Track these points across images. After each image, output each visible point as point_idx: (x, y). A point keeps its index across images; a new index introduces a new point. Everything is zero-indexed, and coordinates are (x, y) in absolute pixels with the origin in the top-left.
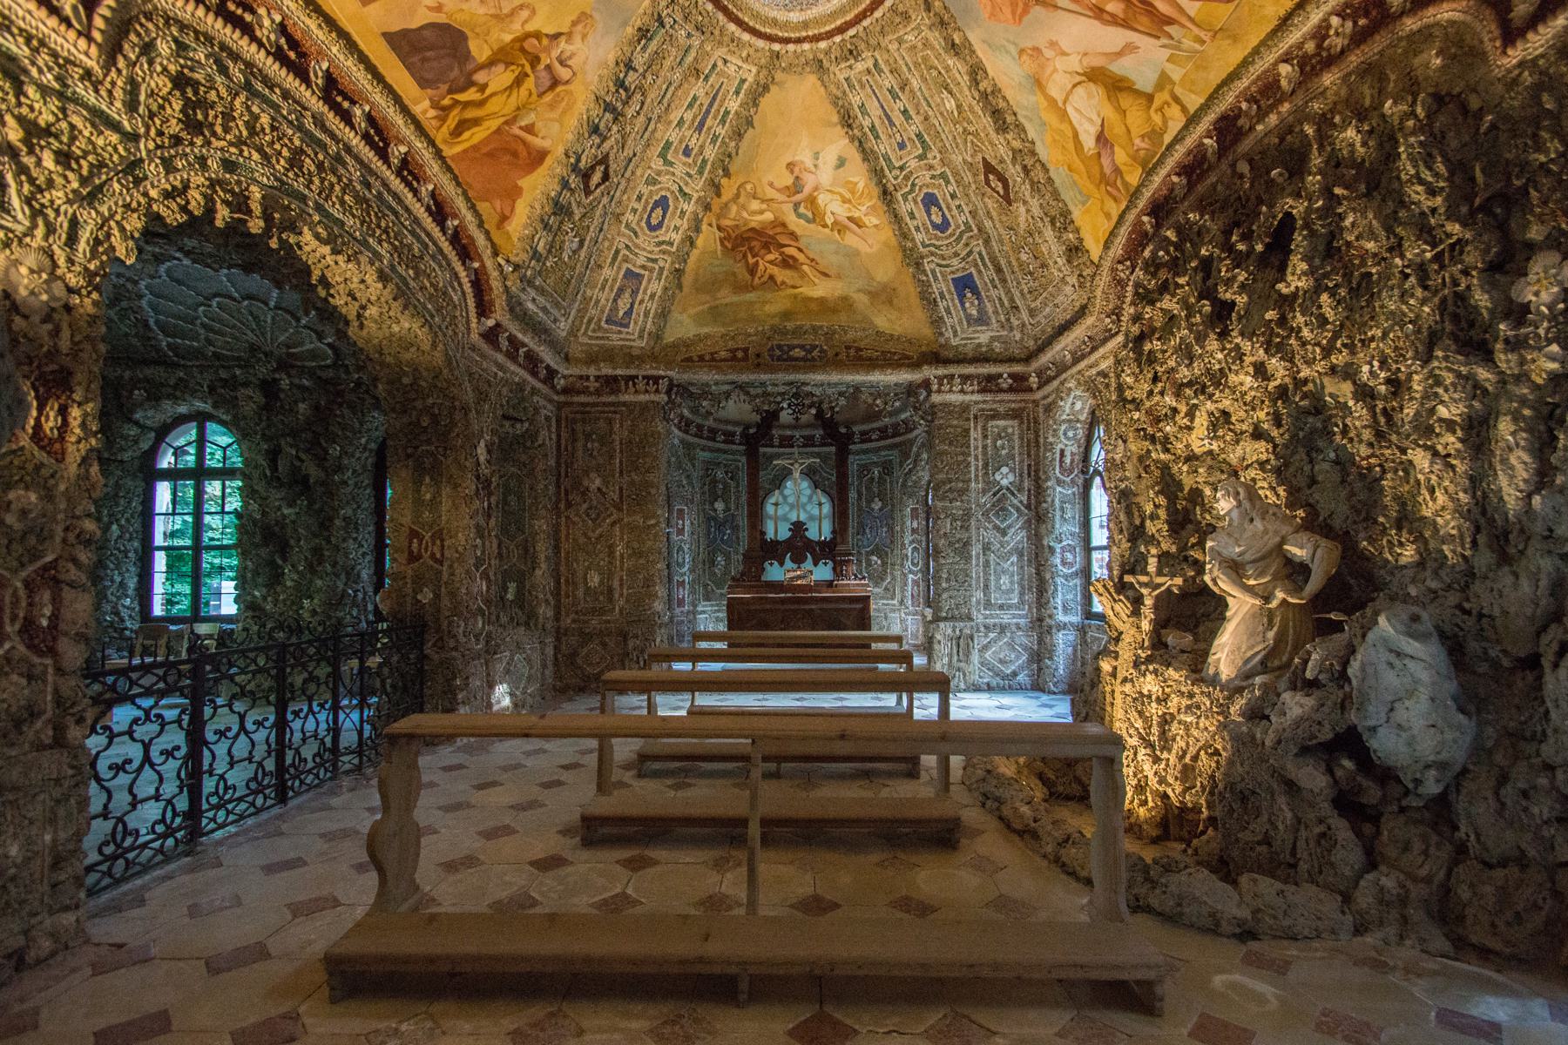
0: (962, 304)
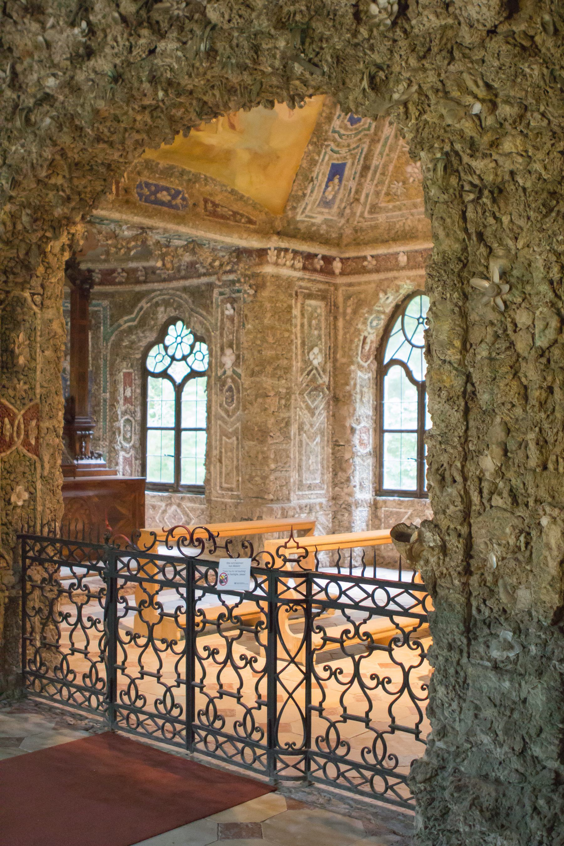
0: (327, 186)
